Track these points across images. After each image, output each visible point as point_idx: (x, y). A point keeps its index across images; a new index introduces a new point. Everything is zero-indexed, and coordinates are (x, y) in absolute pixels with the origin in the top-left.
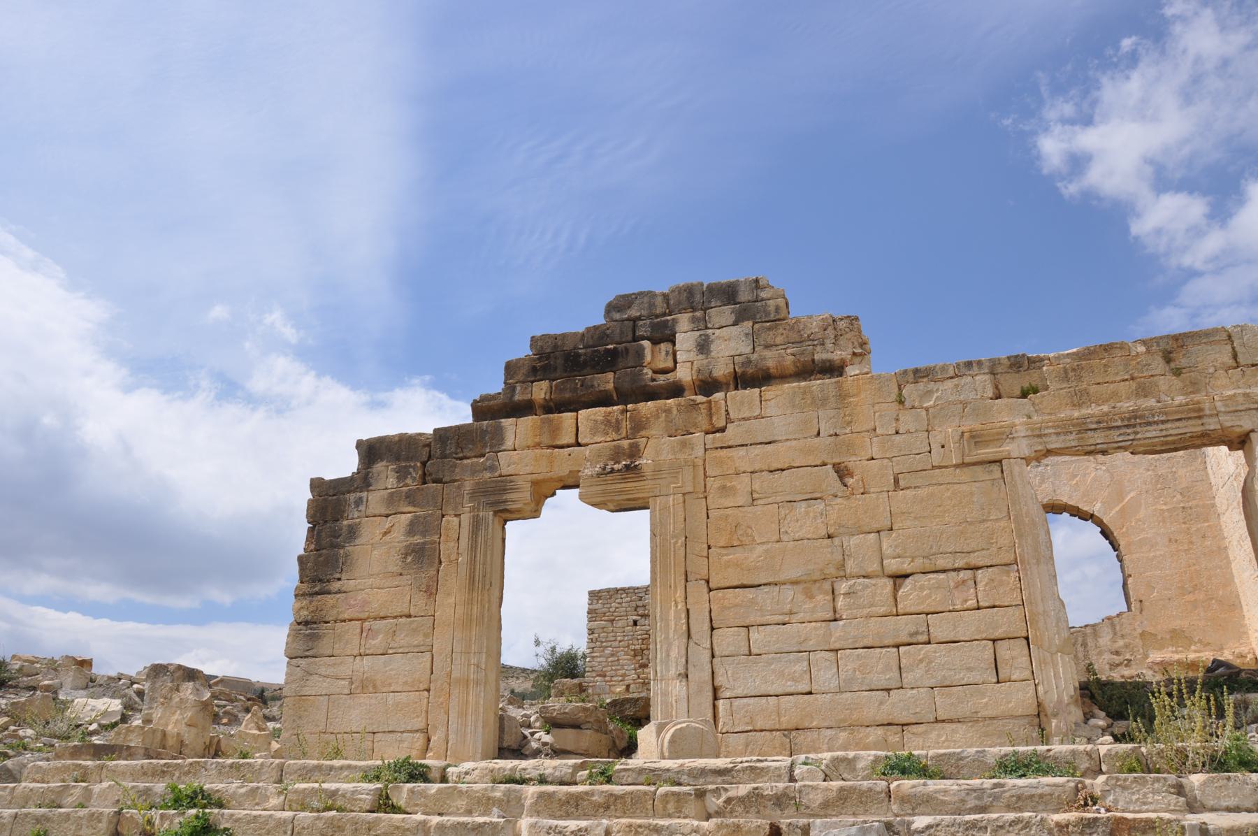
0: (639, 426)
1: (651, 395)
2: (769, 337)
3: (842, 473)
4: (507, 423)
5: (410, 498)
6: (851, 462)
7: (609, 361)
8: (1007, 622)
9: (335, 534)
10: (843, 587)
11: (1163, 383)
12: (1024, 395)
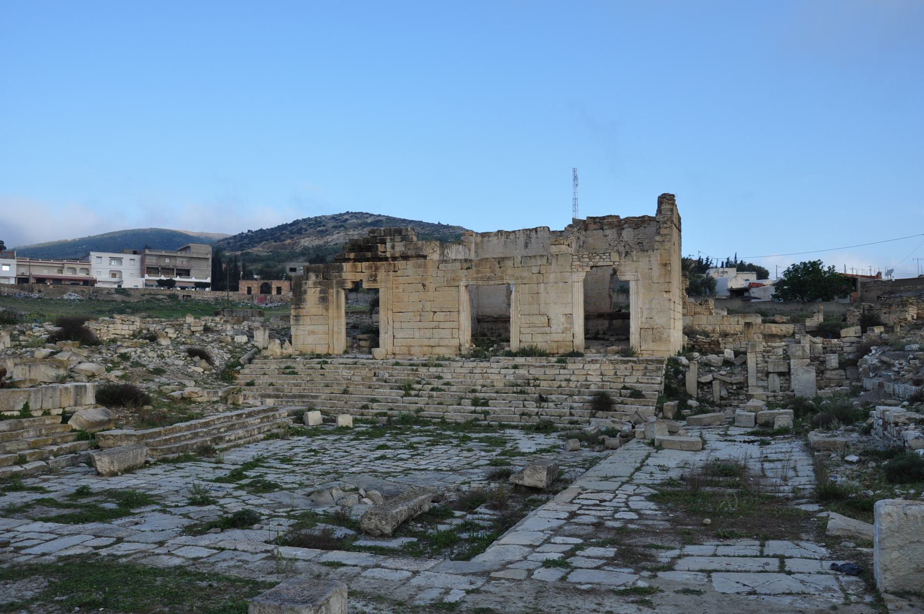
0: (377, 269)
1: (381, 259)
2: (409, 246)
3: (424, 285)
4: (344, 264)
5: (320, 283)
6: (426, 283)
7: (369, 249)
8: (455, 325)
9: (300, 292)
10: (423, 313)
11: (498, 269)
12: (468, 268)
